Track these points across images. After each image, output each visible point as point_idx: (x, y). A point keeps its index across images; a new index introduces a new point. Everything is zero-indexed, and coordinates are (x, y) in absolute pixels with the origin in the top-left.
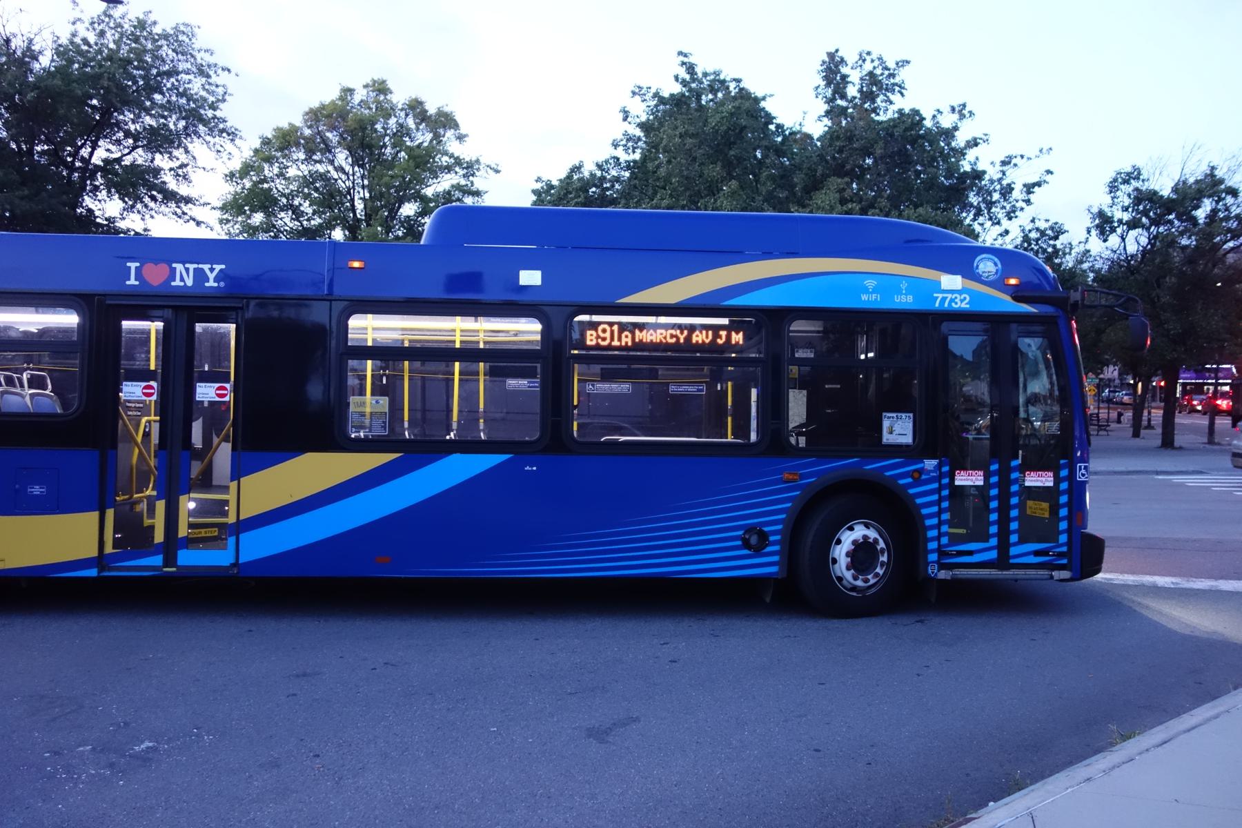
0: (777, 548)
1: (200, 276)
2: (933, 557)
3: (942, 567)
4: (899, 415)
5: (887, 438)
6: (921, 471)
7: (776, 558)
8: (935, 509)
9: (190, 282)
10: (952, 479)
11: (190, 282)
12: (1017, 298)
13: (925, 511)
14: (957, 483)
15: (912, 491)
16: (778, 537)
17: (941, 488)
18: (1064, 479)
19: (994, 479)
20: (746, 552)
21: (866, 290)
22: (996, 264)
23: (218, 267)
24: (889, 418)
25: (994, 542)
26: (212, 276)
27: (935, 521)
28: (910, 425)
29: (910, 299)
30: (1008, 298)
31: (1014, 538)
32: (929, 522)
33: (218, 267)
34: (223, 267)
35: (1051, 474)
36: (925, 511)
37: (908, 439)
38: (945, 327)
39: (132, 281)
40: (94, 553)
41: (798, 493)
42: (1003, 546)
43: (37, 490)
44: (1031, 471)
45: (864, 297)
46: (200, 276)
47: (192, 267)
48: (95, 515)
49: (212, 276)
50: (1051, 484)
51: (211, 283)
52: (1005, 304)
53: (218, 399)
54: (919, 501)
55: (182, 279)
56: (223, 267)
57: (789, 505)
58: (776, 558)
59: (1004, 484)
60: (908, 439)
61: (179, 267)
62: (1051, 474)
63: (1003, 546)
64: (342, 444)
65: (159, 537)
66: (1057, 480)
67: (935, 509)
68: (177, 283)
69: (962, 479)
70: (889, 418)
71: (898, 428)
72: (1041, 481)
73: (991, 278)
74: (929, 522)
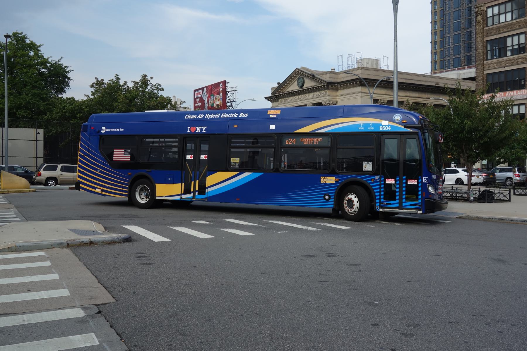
0: (333, 200)
1: (202, 129)
2: (378, 204)
3: (381, 207)
4: (368, 162)
5: (364, 169)
6: (374, 179)
7: (333, 203)
10: (385, 181)
11: (199, 131)
12: (406, 127)
13: (375, 191)
14: (386, 183)
15: (371, 185)
16: (333, 197)
17: (380, 185)
18: (420, 183)
19: (398, 182)
20: (325, 201)
22: (400, 118)
23: (205, 127)
24: (365, 163)
26: (204, 129)
27: (378, 194)
28: (371, 165)
29: (373, 128)
30: (403, 127)
32: (376, 194)
33: (205, 127)
34: (206, 127)
35: (416, 181)
36: (375, 191)
37: (371, 170)
38: (385, 136)
40: (180, 193)
41: (339, 185)
42: (401, 203)
43: (170, 179)
44: (409, 179)
45: (360, 128)
46: (202, 129)
47: (200, 127)
49: (204, 129)
50: (416, 184)
51: (204, 131)
52: (402, 129)
53: (205, 159)
54: (374, 188)
55: (198, 131)
56: (206, 127)
57: (336, 188)
58: (333, 203)
60: (371, 170)
61: (197, 128)
62: (416, 181)
63: (401, 203)
64: (227, 170)
65: (192, 190)
66: (418, 183)
69: (388, 182)
70: (365, 163)
71: (368, 166)
72: (413, 183)
73: (398, 121)
74: (376, 194)
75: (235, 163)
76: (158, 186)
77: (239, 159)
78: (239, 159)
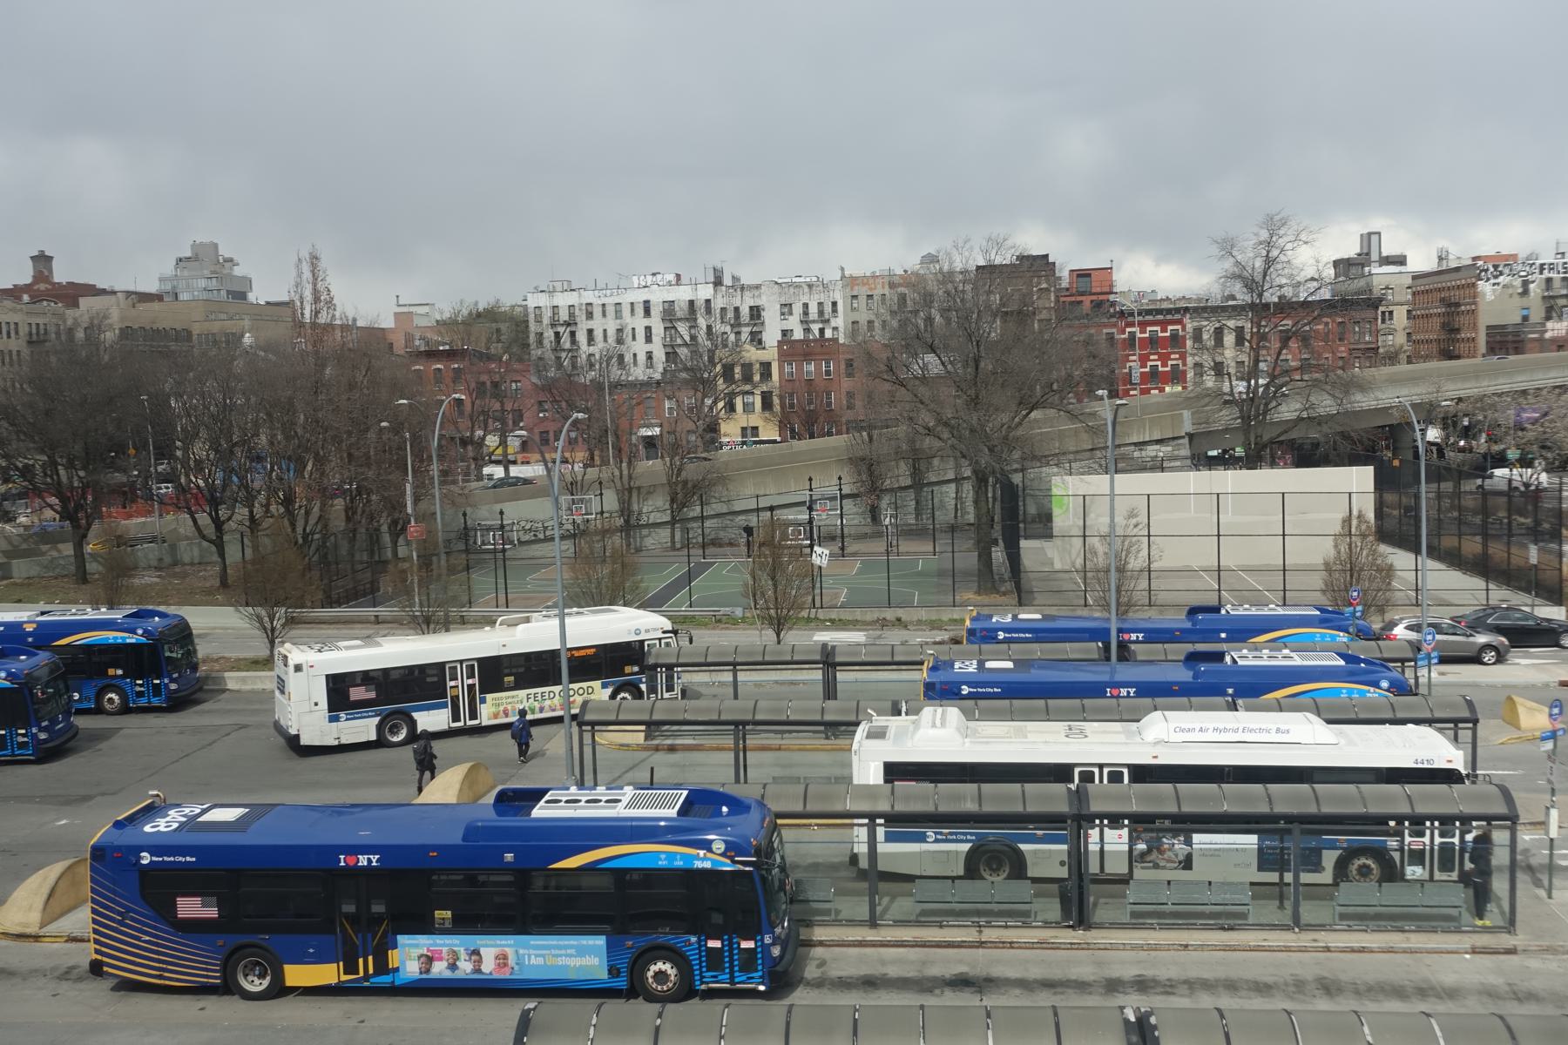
1: (370, 861)
8: (697, 957)
9: (366, 864)
11: (366, 864)
21: (661, 860)
23: (377, 857)
25: (728, 976)
26: (374, 861)
29: (682, 863)
31: (737, 974)
33: (377, 857)
39: (342, 864)
43: (311, 951)
45: (660, 863)
46: (370, 861)
47: (366, 857)
48: (335, 965)
49: (374, 861)
51: (374, 864)
59: (731, 944)
61: (360, 857)
67: (697, 957)
68: (360, 864)
75: (443, 919)
76: (288, 968)
77: (449, 913)
78: (449, 913)
